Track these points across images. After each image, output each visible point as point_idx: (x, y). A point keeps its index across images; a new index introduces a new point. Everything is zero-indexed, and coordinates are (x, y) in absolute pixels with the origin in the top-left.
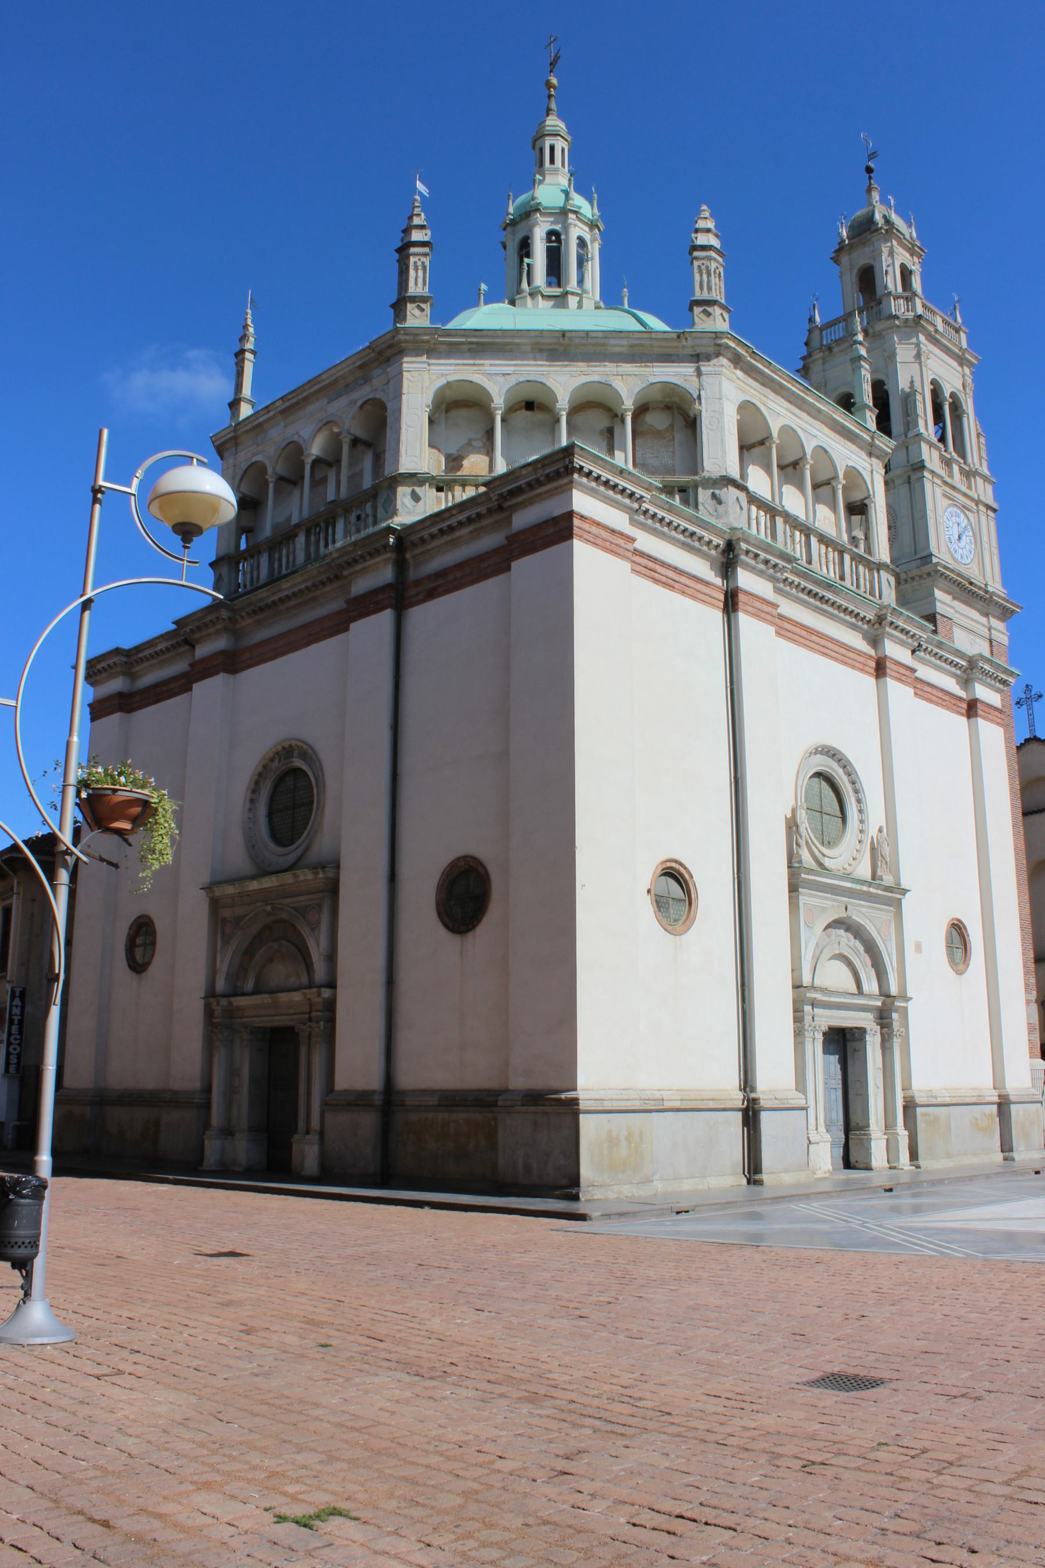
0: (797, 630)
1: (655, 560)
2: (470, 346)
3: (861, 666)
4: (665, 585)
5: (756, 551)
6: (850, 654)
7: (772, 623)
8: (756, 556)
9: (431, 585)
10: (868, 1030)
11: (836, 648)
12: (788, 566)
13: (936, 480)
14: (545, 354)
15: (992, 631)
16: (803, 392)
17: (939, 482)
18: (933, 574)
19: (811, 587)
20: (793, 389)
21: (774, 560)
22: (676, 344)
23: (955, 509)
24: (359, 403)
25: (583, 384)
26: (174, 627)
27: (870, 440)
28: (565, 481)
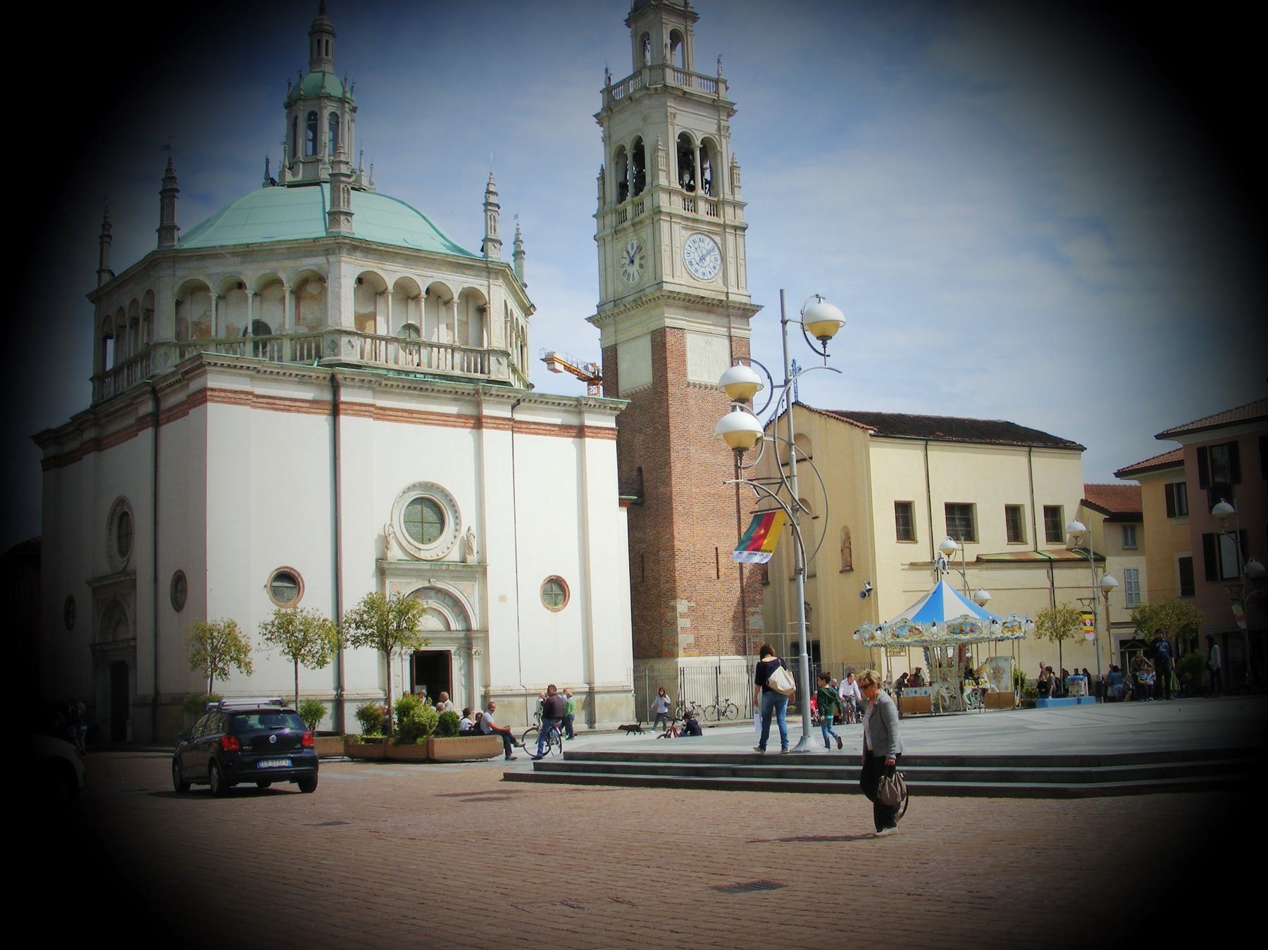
0: (400, 414)
1: (274, 398)
3: (462, 424)
4: (283, 410)
9: (167, 415)
10: (453, 651)
11: (438, 418)
15: (732, 330)
18: (661, 297)
19: (409, 385)
20: (407, 252)
23: (699, 236)
24: (146, 291)
26: (70, 420)
27: (484, 265)
28: (203, 369)
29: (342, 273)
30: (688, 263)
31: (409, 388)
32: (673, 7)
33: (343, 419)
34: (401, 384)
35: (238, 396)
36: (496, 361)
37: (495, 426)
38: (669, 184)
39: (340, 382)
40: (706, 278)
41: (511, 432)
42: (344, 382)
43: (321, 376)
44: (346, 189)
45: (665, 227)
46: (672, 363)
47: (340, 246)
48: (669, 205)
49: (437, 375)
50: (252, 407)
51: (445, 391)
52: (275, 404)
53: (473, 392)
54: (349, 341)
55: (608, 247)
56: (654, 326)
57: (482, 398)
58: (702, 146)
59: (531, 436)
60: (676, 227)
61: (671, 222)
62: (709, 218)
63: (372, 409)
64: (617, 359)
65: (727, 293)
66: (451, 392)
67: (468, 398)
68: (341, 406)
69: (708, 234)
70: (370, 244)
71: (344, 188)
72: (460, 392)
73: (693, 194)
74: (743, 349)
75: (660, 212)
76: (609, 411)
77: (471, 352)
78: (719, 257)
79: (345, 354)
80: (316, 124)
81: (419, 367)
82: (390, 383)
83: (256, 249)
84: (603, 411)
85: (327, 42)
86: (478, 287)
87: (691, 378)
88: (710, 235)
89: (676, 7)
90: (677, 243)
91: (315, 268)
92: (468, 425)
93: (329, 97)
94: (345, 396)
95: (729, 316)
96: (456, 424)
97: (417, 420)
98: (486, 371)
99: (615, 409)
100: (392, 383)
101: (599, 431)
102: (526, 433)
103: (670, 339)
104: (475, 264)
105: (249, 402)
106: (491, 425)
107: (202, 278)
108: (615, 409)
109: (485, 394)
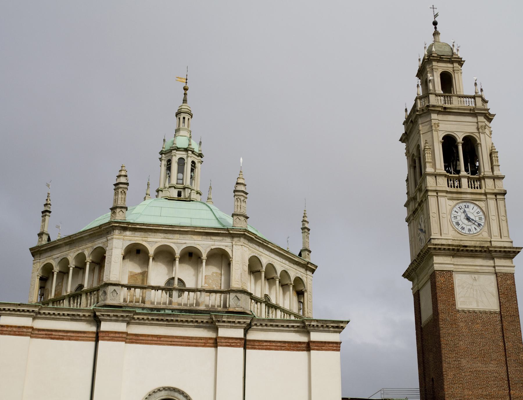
0: (150, 338)
2: (50, 249)
3: (203, 344)
5: (107, 313)
6: (194, 341)
7: (122, 341)
8: (109, 315)
12: (130, 315)
13: (439, 194)
14: (69, 246)
15: (496, 268)
16: (170, 227)
17: (444, 194)
19: (157, 318)
21: (119, 314)
22: (100, 230)
23: (465, 204)
25: (78, 254)
29: (113, 246)
30: (455, 224)
31: (157, 320)
32: (440, 58)
33: (101, 343)
34: (150, 317)
35: (21, 330)
36: (236, 298)
37: (228, 344)
38: (435, 171)
39: (100, 318)
40: (472, 233)
41: (242, 349)
42: (102, 317)
43: (87, 314)
44: (123, 192)
45: (432, 201)
46: (441, 297)
47: (114, 228)
48: (435, 185)
49: (183, 310)
50: (31, 337)
51: (187, 321)
52: (52, 335)
53: (210, 321)
54: (115, 290)
55: (412, 224)
56: (430, 272)
57: (217, 324)
58: (463, 142)
59: (264, 351)
60: (442, 200)
61: (437, 197)
62: (470, 190)
63: (124, 336)
64: (419, 300)
65: (491, 242)
66: (192, 321)
67: (208, 325)
68: (100, 335)
69: (472, 201)
70: (135, 225)
71: (121, 192)
72: (199, 321)
73: (457, 175)
74: (508, 282)
75: (427, 191)
76: (331, 329)
77: (216, 293)
78: (483, 217)
79: (111, 299)
80: (170, 166)
81: (170, 306)
82: (141, 317)
83: (74, 238)
84: (327, 329)
85: (184, 118)
86: (223, 248)
87: (460, 306)
88: (474, 202)
89: (442, 57)
90: (443, 210)
91: (101, 245)
92: (208, 345)
93: (178, 149)
94: (105, 326)
95: (493, 258)
96: (197, 344)
97: (164, 343)
98: (228, 306)
99: (337, 327)
100: (142, 317)
101: (321, 345)
102: (259, 349)
103: (440, 280)
104: (219, 232)
105: (29, 334)
106: (224, 344)
107: (51, 261)
108: (337, 327)
109: (219, 321)
